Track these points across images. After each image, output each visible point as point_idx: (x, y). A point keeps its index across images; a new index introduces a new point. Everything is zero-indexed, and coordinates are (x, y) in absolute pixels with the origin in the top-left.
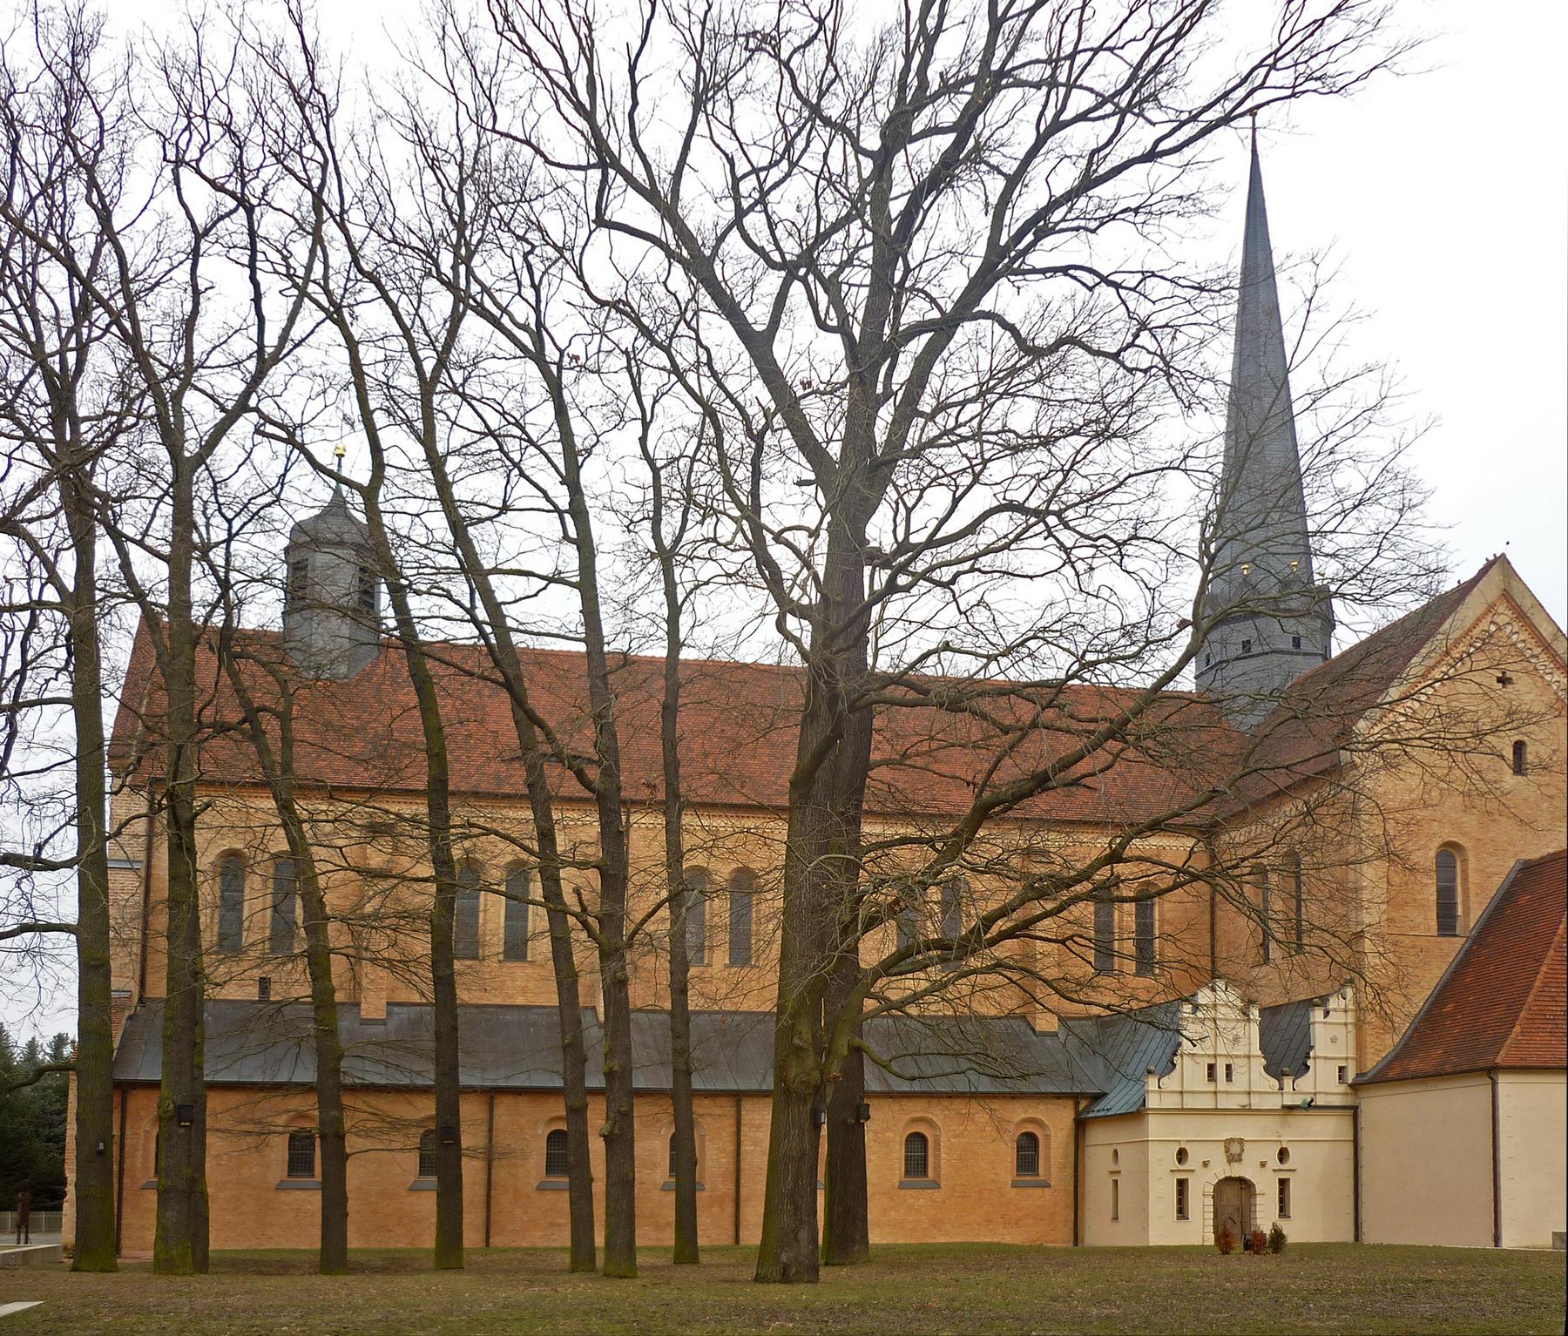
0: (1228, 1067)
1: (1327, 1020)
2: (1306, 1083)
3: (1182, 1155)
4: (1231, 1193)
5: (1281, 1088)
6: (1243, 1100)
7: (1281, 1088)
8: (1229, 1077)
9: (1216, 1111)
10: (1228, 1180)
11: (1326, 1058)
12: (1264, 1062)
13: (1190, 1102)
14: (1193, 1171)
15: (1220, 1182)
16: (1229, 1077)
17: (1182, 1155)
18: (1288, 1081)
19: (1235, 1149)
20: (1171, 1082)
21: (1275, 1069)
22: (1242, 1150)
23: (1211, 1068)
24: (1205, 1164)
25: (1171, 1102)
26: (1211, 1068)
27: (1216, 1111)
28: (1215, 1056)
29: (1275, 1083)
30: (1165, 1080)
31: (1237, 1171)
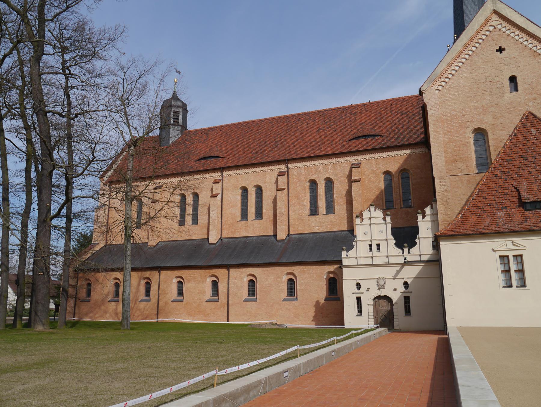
0: (378, 245)
1: (424, 220)
2: (415, 250)
3: (358, 286)
4: (384, 302)
5: (403, 253)
6: (385, 260)
7: (403, 253)
8: (379, 249)
9: (373, 265)
10: (379, 298)
11: (424, 238)
12: (394, 242)
13: (361, 262)
14: (363, 293)
15: (375, 298)
16: (379, 249)
17: (358, 286)
18: (406, 250)
19: (381, 282)
20: (352, 253)
21: (399, 245)
22: (385, 283)
23: (370, 246)
24: (368, 290)
25: (353, 262)
26: (370, 246)
27: (373, 265)
28: (371, 241)
29: (400, 251)
30: (349, 252)
31: (383, 293)
